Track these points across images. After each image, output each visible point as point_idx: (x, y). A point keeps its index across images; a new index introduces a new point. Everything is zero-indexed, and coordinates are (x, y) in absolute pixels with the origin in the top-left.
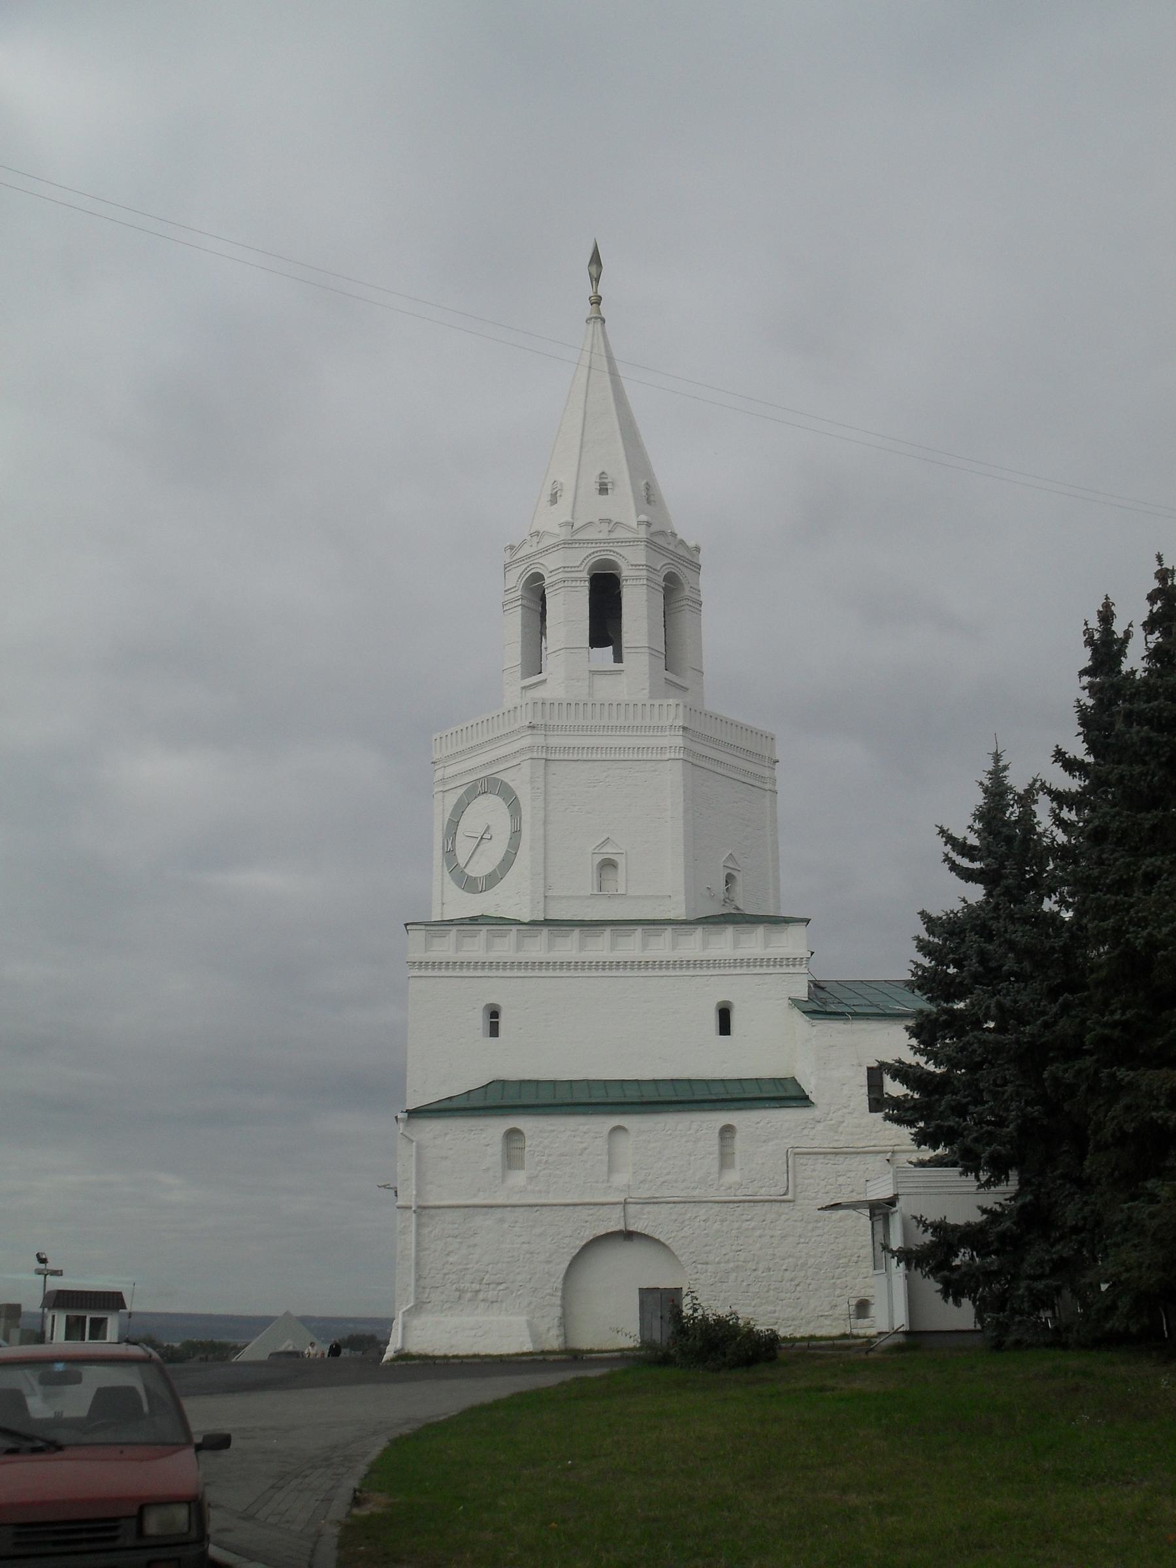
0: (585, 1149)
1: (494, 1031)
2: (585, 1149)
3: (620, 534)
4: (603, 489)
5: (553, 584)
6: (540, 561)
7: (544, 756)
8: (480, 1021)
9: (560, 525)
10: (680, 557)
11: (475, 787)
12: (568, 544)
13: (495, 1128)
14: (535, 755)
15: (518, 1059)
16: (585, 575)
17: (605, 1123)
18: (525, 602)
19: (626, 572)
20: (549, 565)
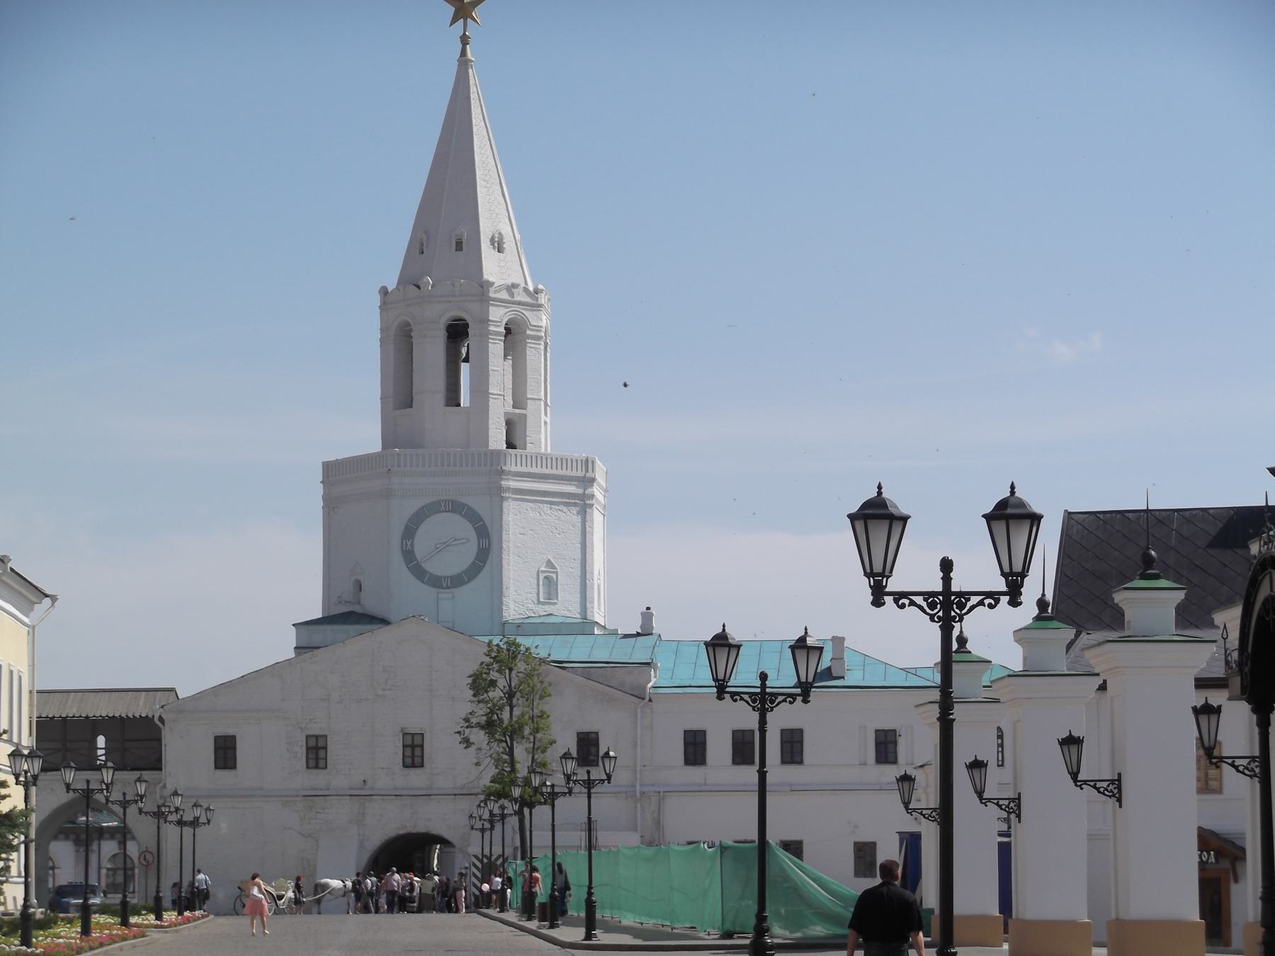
4: (459, 246)
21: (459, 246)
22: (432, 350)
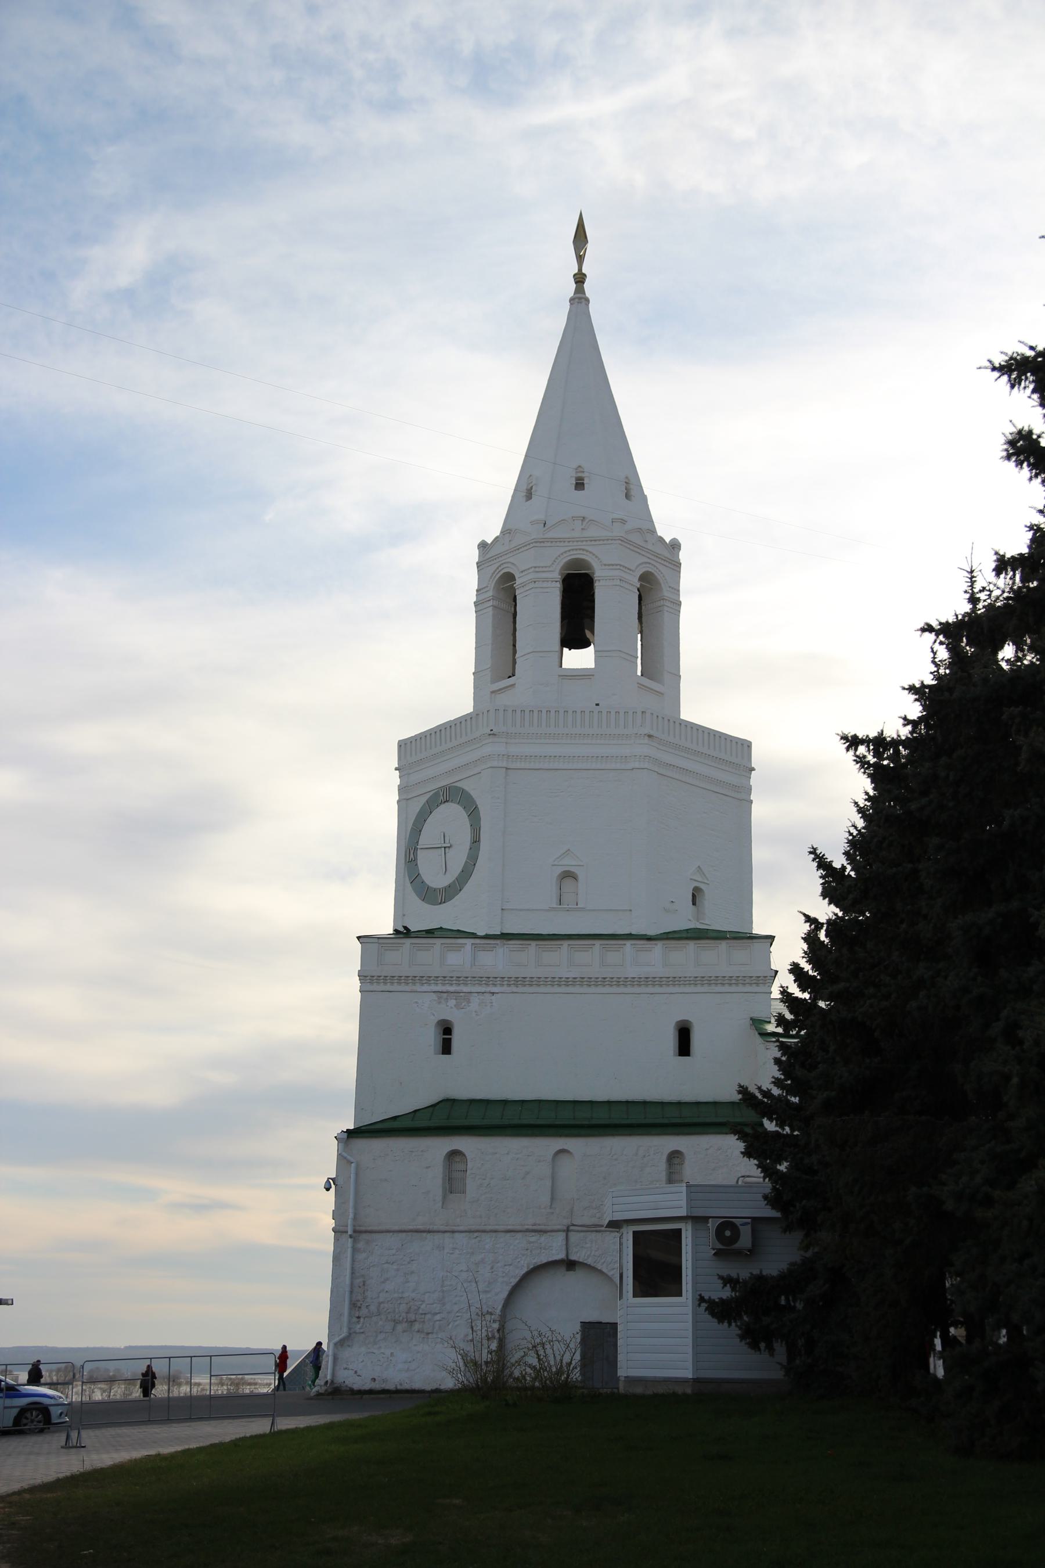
0: (528, 1173)
1: (446, 1048)
2: (528, 1173)
3: (592, 532)
4: (580, 485)
5: (523, 585)
6: (511, 560)
7: (504, 764)
8: (431, 1037)
9: (532, 523)
10: (657, 555)
11: (436, 795)
12: (540, 542)
13: (439, 1146)
14: (495, 764)
15: (470, 1077)
16: (557, 575)
17: (547, 1146)
18: (496, 603)
19: (599, 574)
20: (521, 565)
21: (580, 485)
22: (542, 608)
